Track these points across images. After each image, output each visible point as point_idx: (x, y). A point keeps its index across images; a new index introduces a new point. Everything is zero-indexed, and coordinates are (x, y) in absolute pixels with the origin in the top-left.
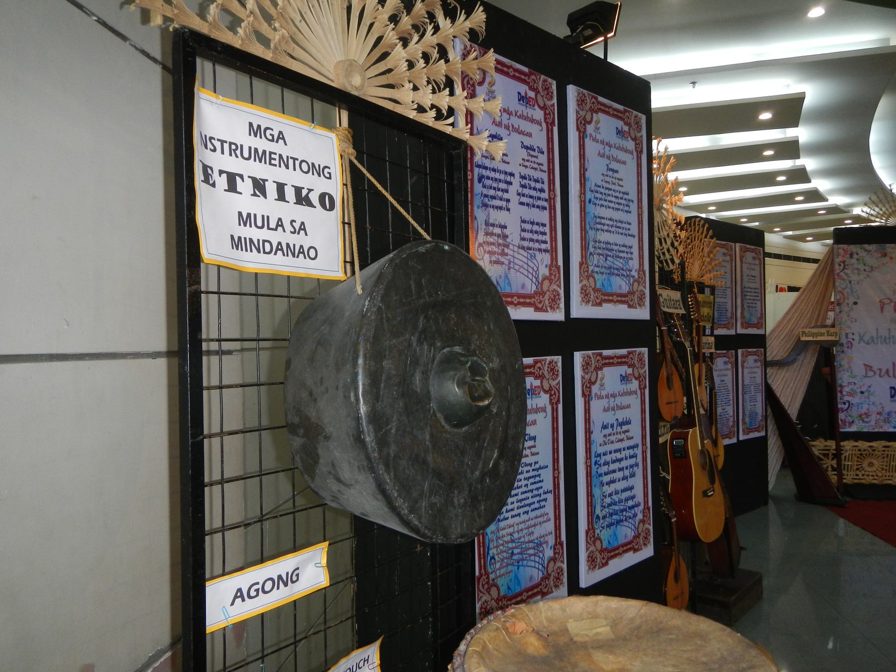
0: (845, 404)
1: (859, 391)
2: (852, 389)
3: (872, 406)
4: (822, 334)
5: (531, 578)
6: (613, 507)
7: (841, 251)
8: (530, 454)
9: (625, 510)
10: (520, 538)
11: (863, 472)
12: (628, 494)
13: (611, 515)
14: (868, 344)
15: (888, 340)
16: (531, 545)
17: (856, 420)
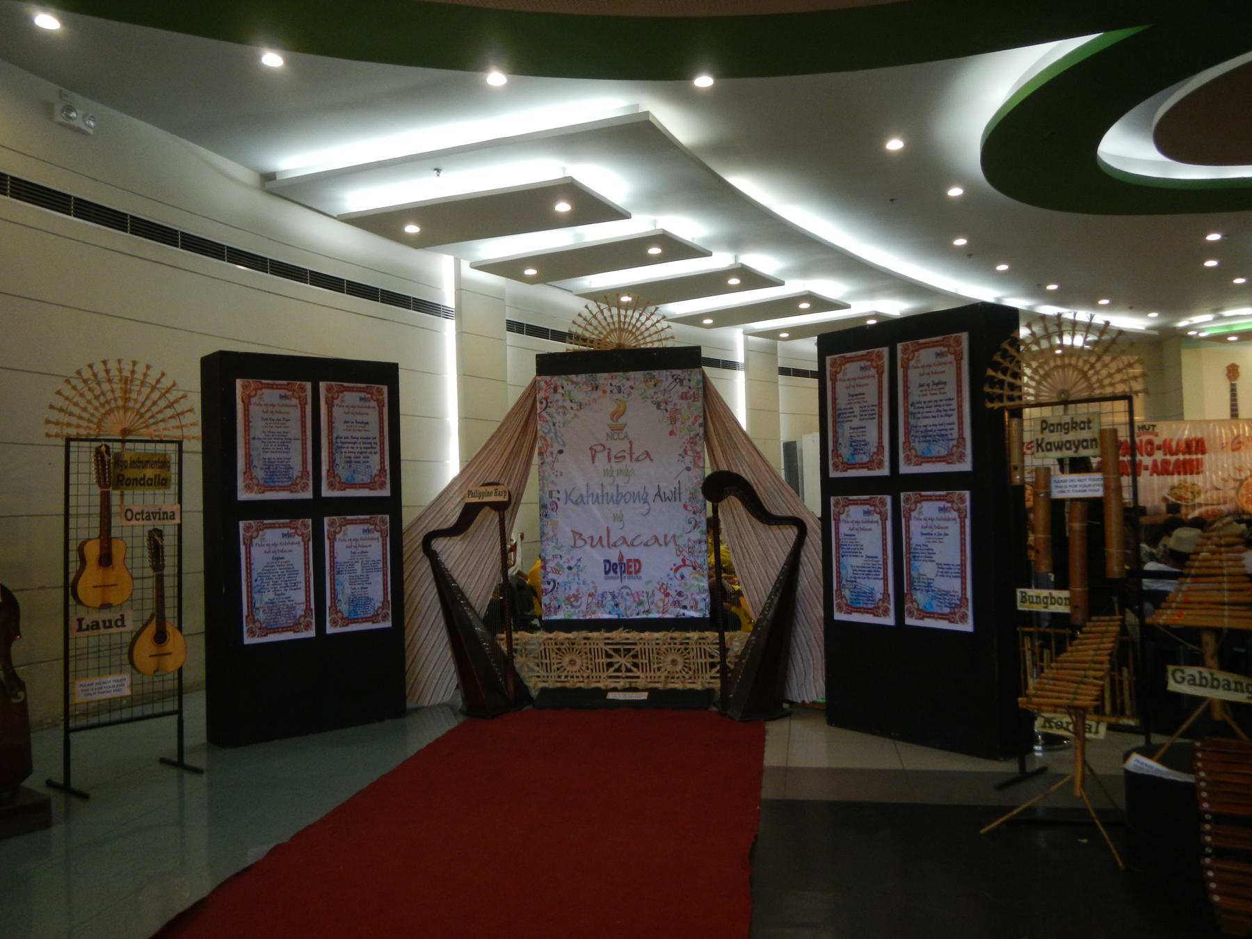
0: (549, 583)
1: (566, 566)
2: (558, 564)
3: (582, 586)
4: (489, 494)
7: (542, 384)
11: (565, 673)
14: (576, 503)
15: (600, 498)
17: (563, 604)
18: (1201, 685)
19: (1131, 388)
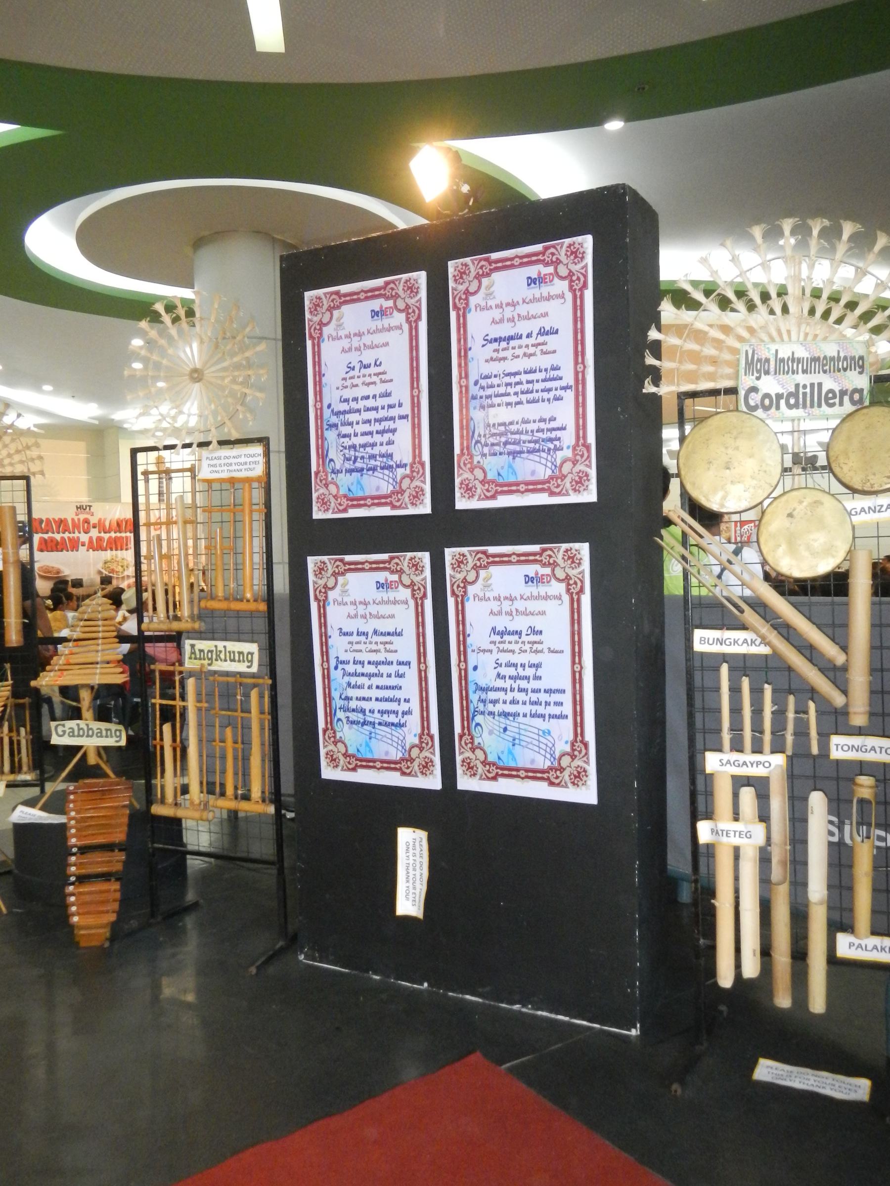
18: (79, 736)
19: (29, 469)
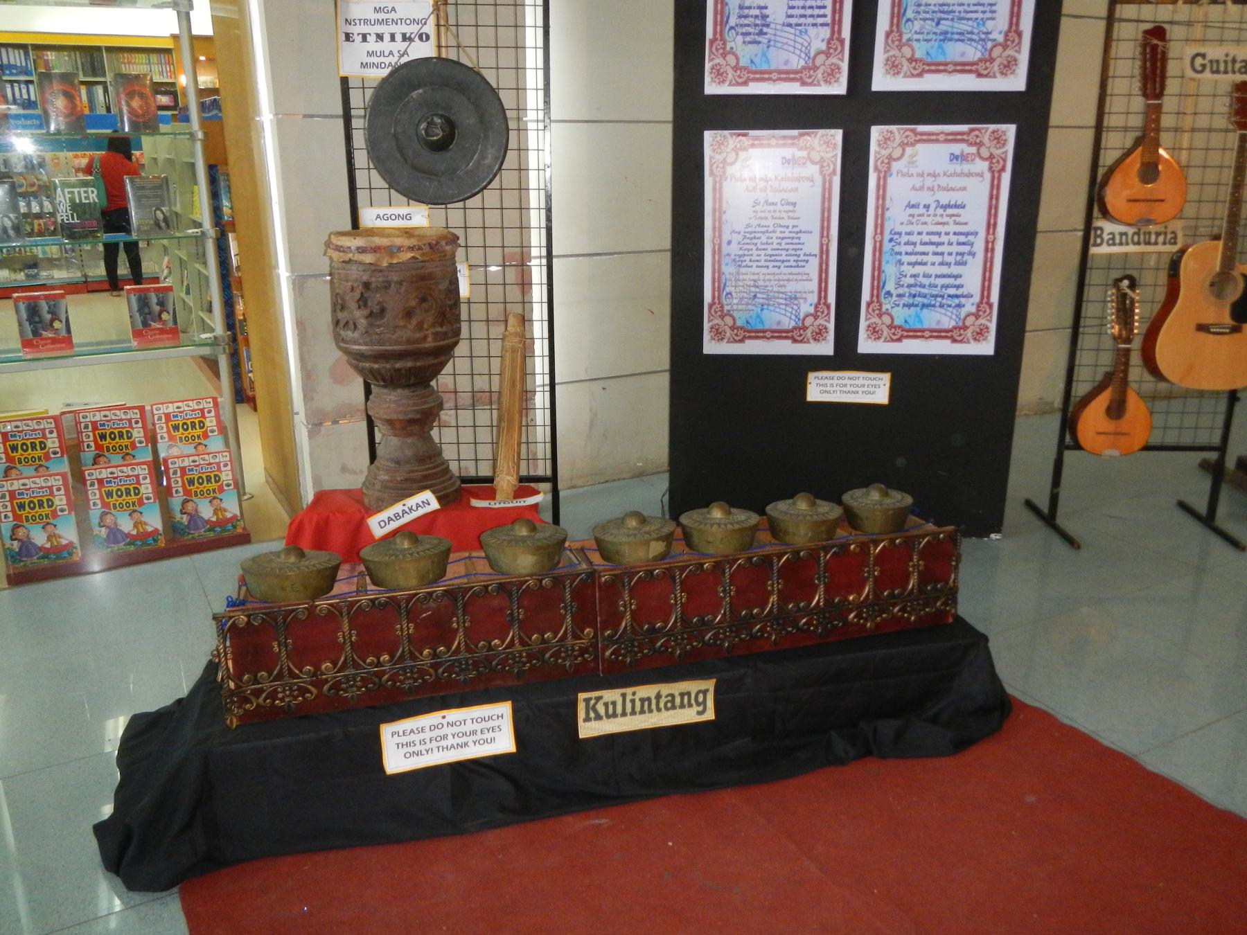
5: (779, 323)
6: (918, 289)
8: (786, 218)
9: (942, 297)
10: (767, 286)
12: (951, 281)
13: (914, 296)
16: (781, 295)
